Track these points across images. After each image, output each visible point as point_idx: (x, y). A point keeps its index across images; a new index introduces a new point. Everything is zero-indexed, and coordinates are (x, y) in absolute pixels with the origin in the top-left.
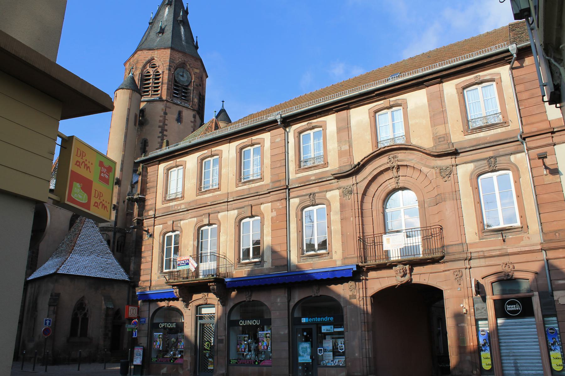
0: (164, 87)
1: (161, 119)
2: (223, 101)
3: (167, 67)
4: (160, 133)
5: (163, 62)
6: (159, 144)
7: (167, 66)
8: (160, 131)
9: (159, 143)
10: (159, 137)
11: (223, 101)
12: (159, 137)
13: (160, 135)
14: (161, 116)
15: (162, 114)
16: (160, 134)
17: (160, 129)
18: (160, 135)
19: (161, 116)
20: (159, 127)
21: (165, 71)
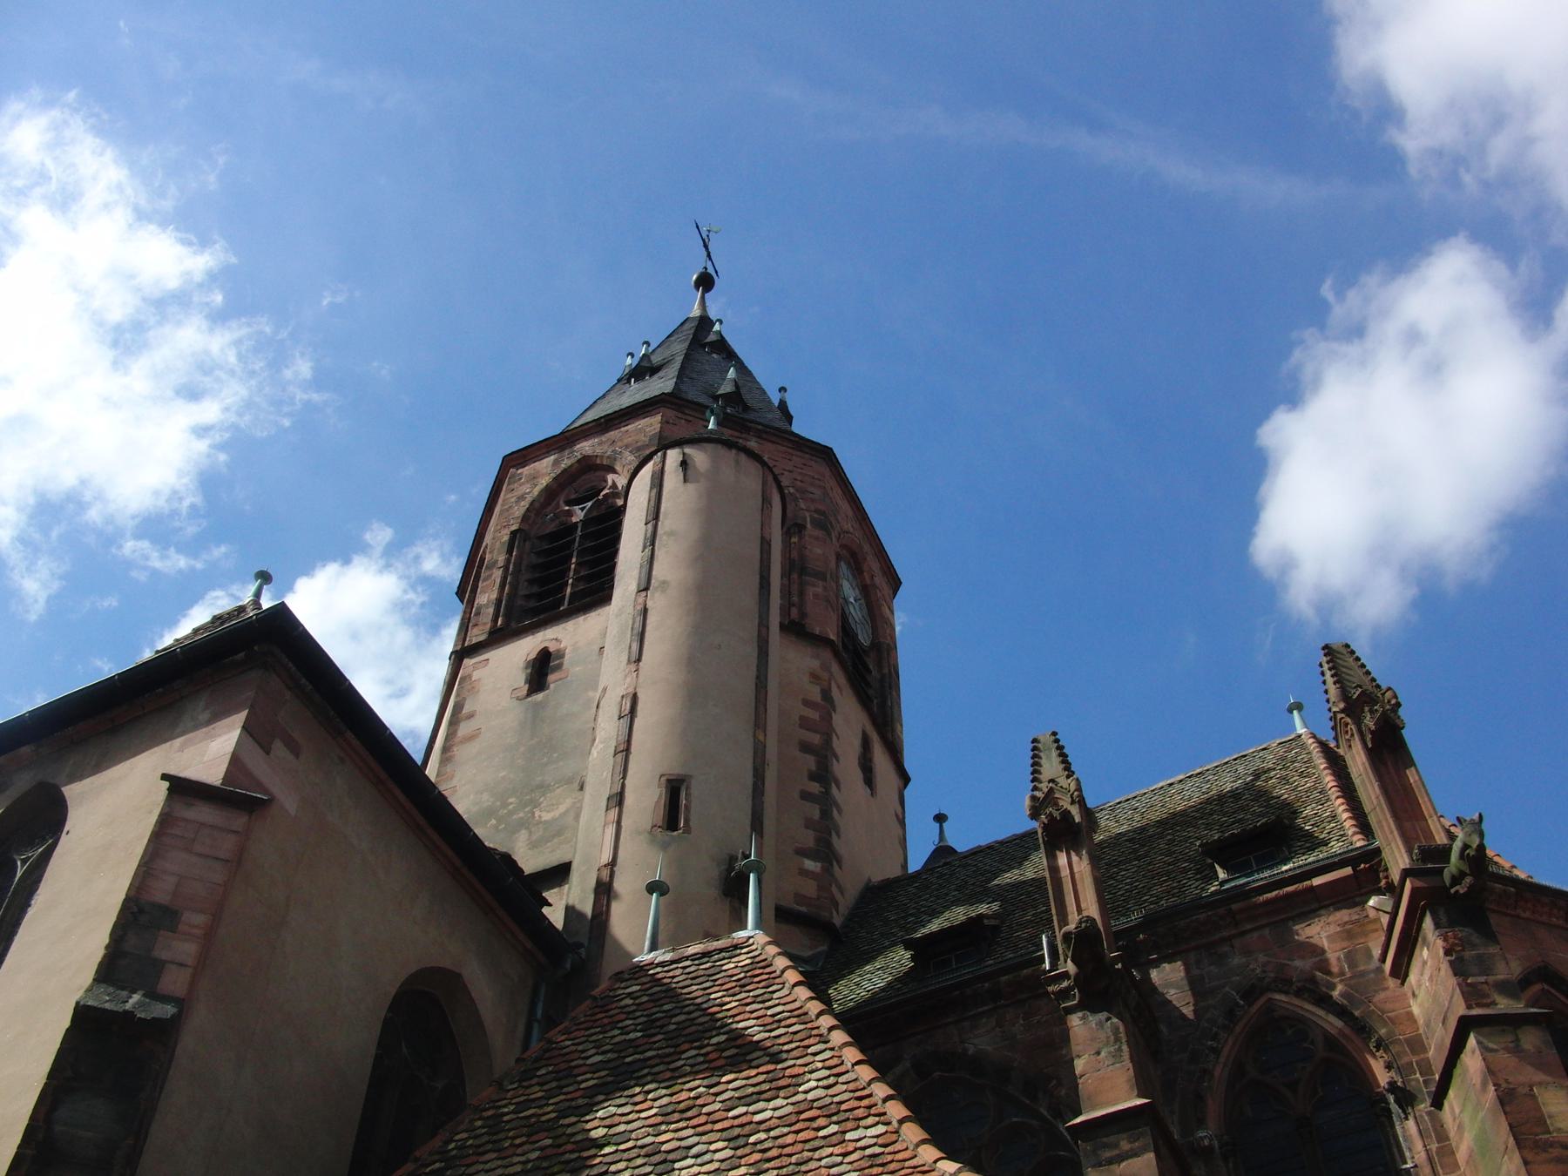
0: (814, 586)
1: (814, 715)
2: (940, 818)
3: (816, 516)
4: (813, 777)
5: (792, 490)
6: (811, 832)
7: (816, 511)
8: (813, 767)
9: (809, 824)
10: (806, 796)
11: (940, 818)
12: (806, 796)
13: (817, 792)
14: (807, 703)
15: (815, 694)
16: (817, 785)
17: (810, 762)
18: (815, 788)
19: (807, 703)
20: (806, 748)
21: (809, 526)
